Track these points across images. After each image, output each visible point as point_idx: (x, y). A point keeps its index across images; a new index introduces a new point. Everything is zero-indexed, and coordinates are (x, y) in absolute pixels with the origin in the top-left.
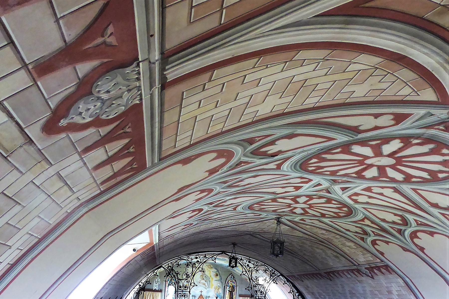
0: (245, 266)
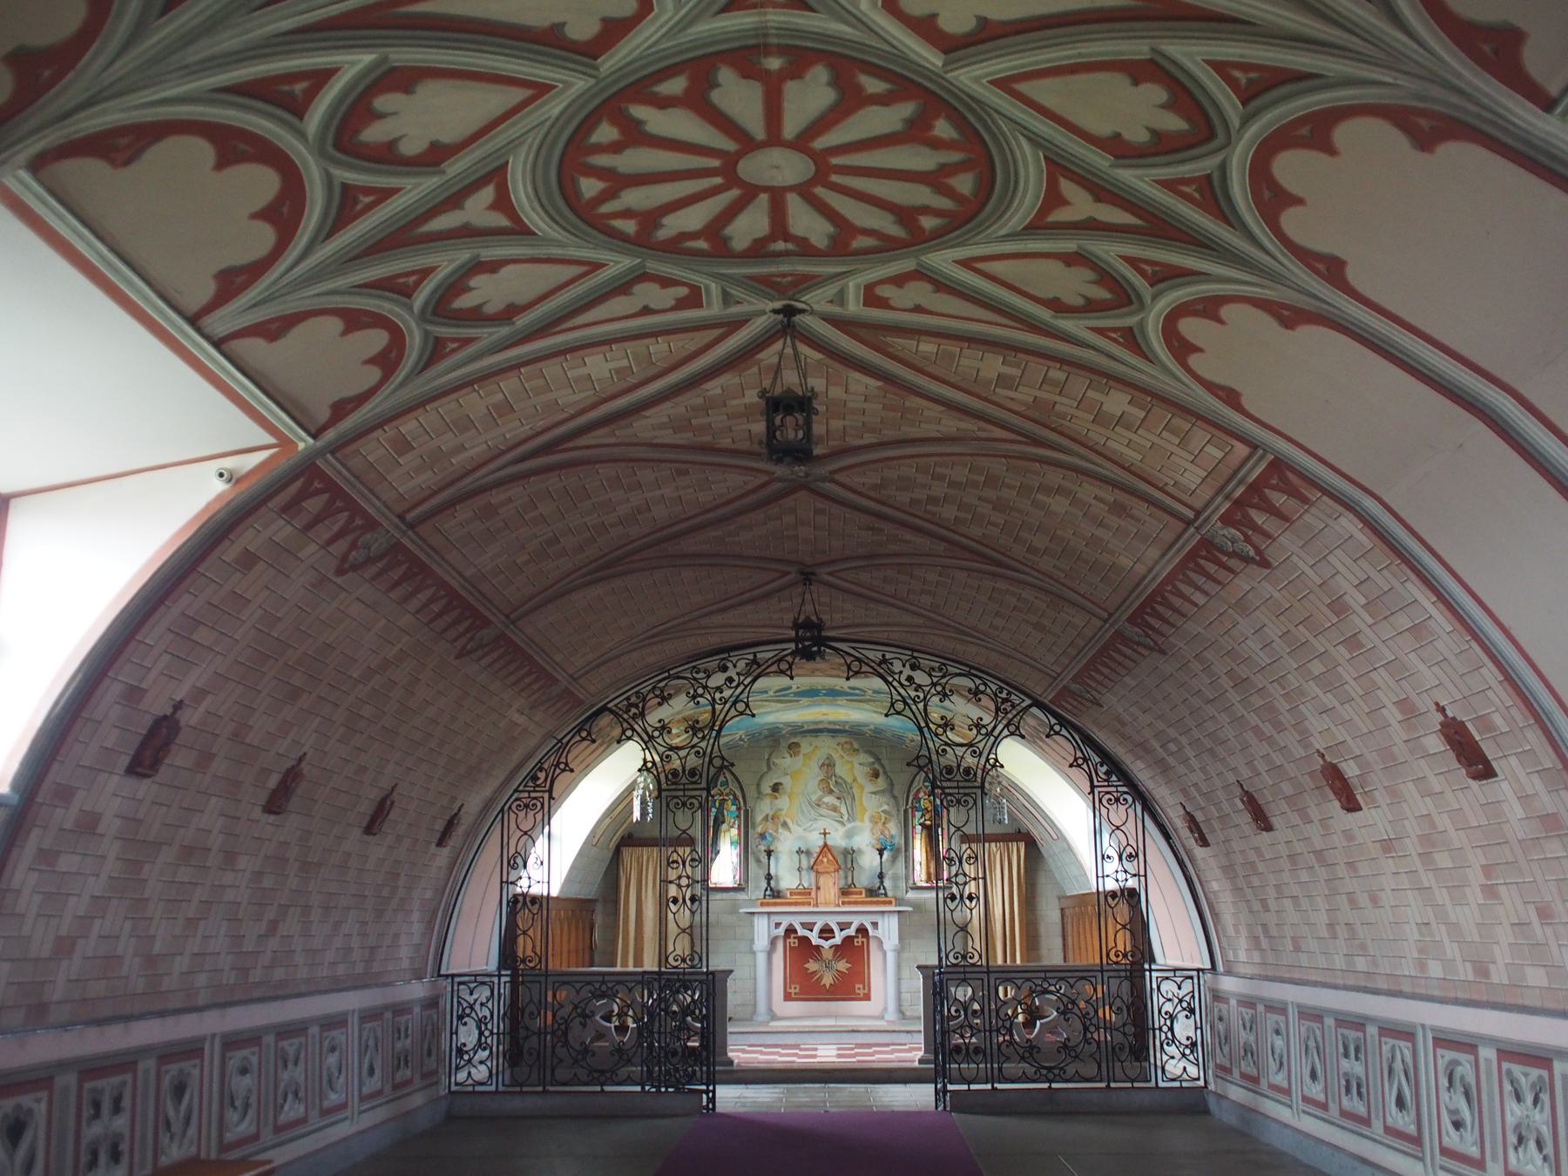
0: (900, 682)
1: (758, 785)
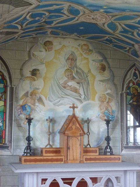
1: (21, 70)
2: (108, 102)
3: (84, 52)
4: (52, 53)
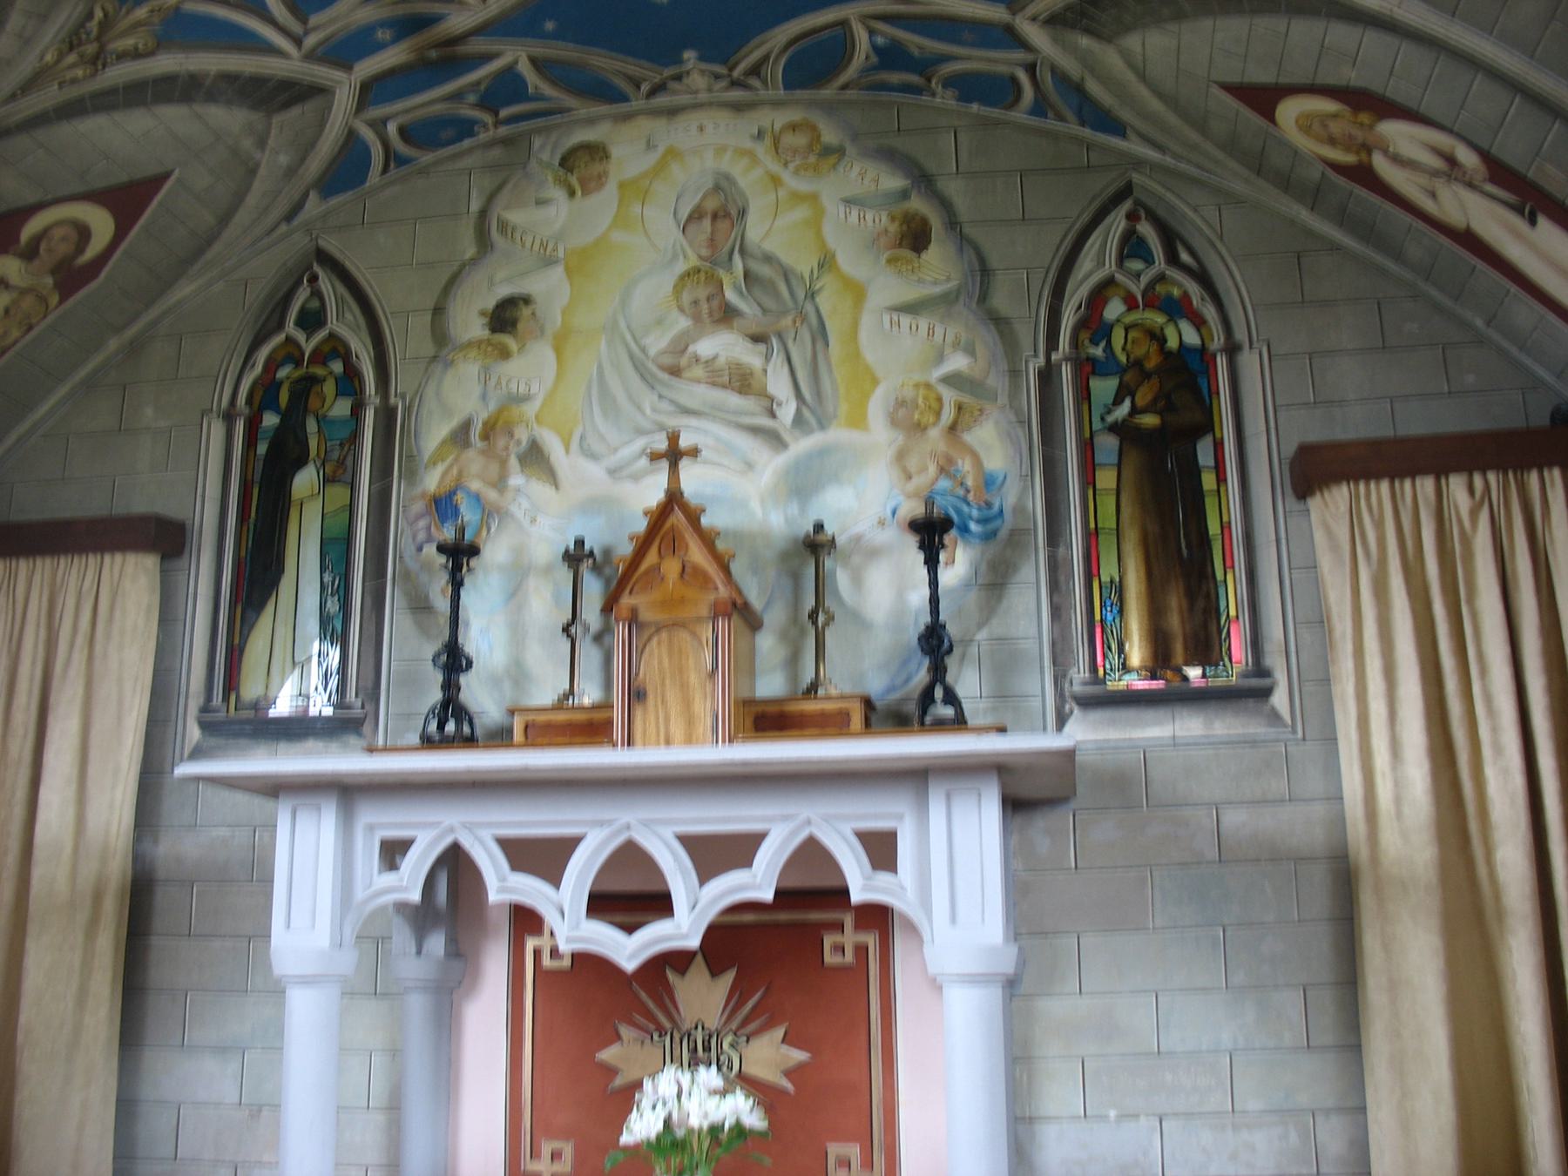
1: (439, 311)
2: (953, 428)
3: (791, 166)
4: (603, 203)
